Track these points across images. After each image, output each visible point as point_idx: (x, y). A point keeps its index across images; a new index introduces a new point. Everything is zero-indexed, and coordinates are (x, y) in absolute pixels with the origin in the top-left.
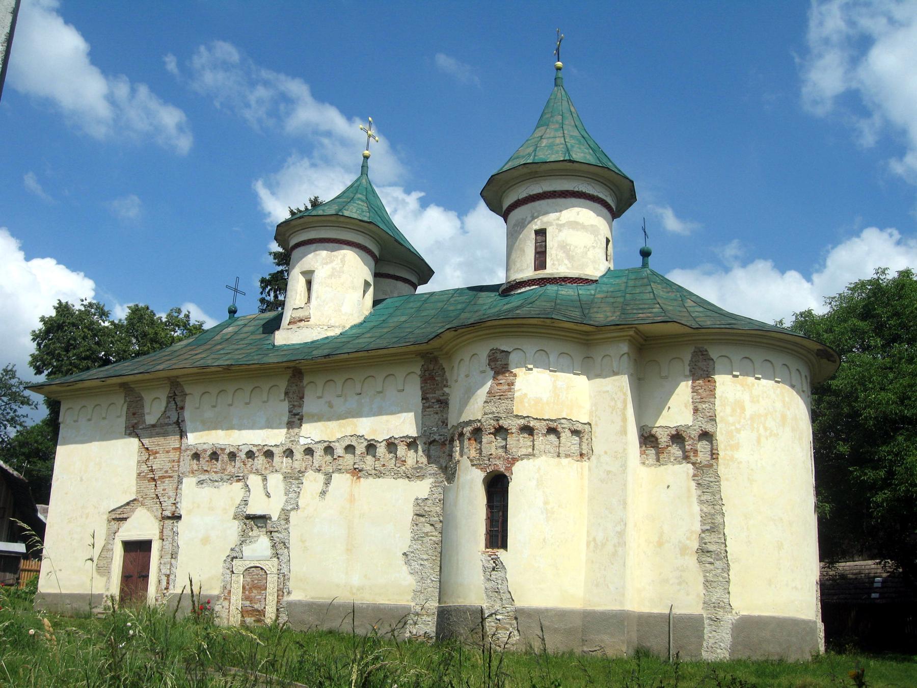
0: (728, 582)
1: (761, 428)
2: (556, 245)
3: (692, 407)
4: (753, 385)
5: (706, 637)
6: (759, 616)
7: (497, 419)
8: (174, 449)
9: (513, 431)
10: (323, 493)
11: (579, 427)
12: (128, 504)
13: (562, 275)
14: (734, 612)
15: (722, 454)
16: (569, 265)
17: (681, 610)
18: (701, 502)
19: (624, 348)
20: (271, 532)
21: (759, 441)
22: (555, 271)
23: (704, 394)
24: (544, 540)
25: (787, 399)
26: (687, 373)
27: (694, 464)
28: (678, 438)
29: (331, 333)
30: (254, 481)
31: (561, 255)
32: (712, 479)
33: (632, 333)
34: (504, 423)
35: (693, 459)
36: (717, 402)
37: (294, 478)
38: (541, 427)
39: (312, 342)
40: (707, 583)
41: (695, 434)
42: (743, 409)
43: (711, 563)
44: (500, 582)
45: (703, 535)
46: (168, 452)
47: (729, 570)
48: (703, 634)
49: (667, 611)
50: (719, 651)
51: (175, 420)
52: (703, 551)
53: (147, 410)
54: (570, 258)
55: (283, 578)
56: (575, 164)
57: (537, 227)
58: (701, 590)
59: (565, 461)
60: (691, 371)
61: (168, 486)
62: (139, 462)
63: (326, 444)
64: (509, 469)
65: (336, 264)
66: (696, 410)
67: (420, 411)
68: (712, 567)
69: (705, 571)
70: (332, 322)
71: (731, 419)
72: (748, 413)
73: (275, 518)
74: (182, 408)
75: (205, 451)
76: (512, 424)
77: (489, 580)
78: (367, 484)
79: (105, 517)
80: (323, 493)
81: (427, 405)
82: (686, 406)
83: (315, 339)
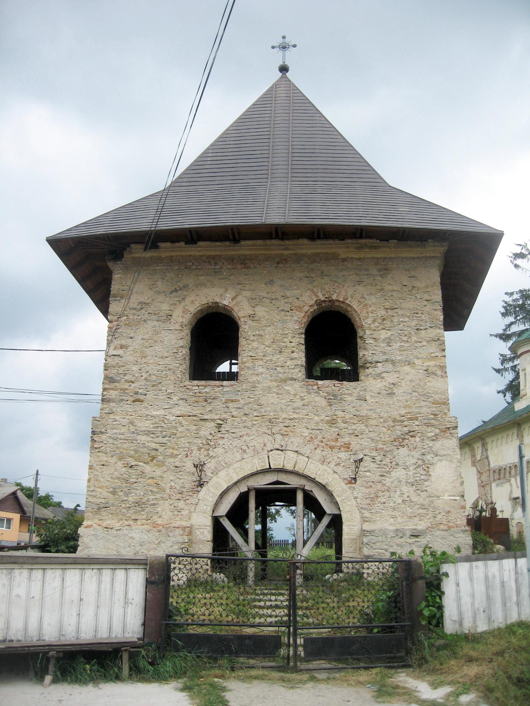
30: (513, 480)
39: (527, 407)
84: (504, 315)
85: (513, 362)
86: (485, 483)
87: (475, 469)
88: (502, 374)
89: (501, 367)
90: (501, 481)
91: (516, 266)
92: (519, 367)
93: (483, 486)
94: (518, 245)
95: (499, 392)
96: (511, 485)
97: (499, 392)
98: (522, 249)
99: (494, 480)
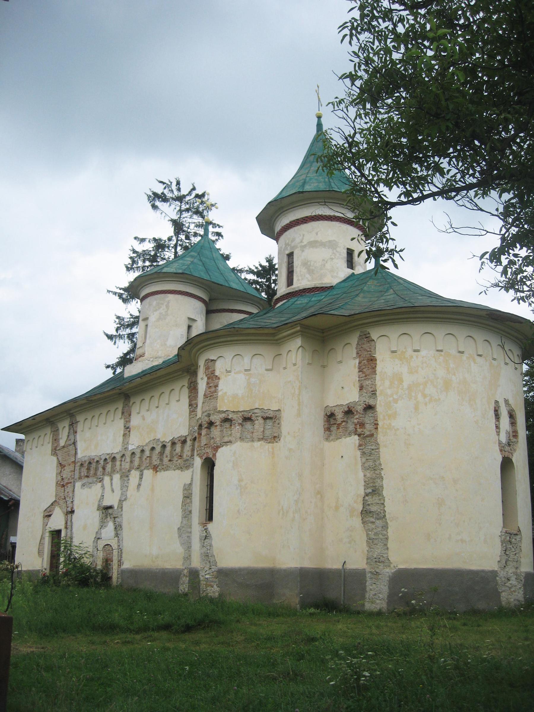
0: (387, 539)
1: (420, 396)
2: (300, 264)
3: (357, 385)
4: (412, 357)
5: (368, 589)
6: (415, 569)
7: (209, 415)
8: (72, 462)
9: (217, 424)
10: (139, 485)
11: (271, 414)
12: (52, 504)
13: (301, 288)
14: (392, 566)
15: (380, 423)
16: (310, 278)
17: (351, 566)
18: (365, 468)
19: (298, 342)
20: (115, 518)
21: (416, 408)
22: (299, 285)
23: (367, 373)
24: (238, 511)
25: (452, 365)
26: (355, 355)
27: (359, 435)
28: (349, 412)
29: (155, 363)
30: (107, 479)
31: (304, 270)
32: (373, 448)
33: (299, 328)
34: (213, 418)
35: (359, 430)
36: (378, 377)
37: (125, 476)
38: (237, 418)
40: (371, 542)
41: (360, 408)
42: (401, 380)
43: (373, 523)
44: (208, 547)
45: (367, 498)
46: (70, 465)
47: (388, 528)
48: (365, 586)
49: (340, 567)
50: (378, 601)
51: (72, 441)
52: (366, 513)
53: (60, 437)
54: (311, 272)
55: (120, 551)
56: (305, 194)
57: (287, 252)
58: (364, 547)
59: (257, 444)
60: (357, 353)
61: (69, 488)
62: (57, 474)
63: (141, 448)
64: (214, 455)
65: (163, 310)
66: (361, 388)
67: (188, 415)
68: (373, 526)
69: (367, 531)
70: (160, 354)
71: (389, 392)
72: (405, 385)
73: (116, 508)
74: (76, 432)
75: (85, 461)
76: (216, 418)
77: (203, 546)
78: (163, 475)
79: (42, 515)
80: (139, 485)
81: (191, 410)
82: (354, 385)
83: (144, 369)
84: (128, 269)
85: (131, 329)
86: (66, 481)
87: (55, 459)
88: (115, 343)
89: (115, 333)
90: (90, 480)
91: (154, 207)
92: (137, 336)
93: (63, 486)
94: (161, 182)
95: (108, 367)
96: (103, 486)
97: (108, 367)
98: (165, 188)
99: (80, 478)
